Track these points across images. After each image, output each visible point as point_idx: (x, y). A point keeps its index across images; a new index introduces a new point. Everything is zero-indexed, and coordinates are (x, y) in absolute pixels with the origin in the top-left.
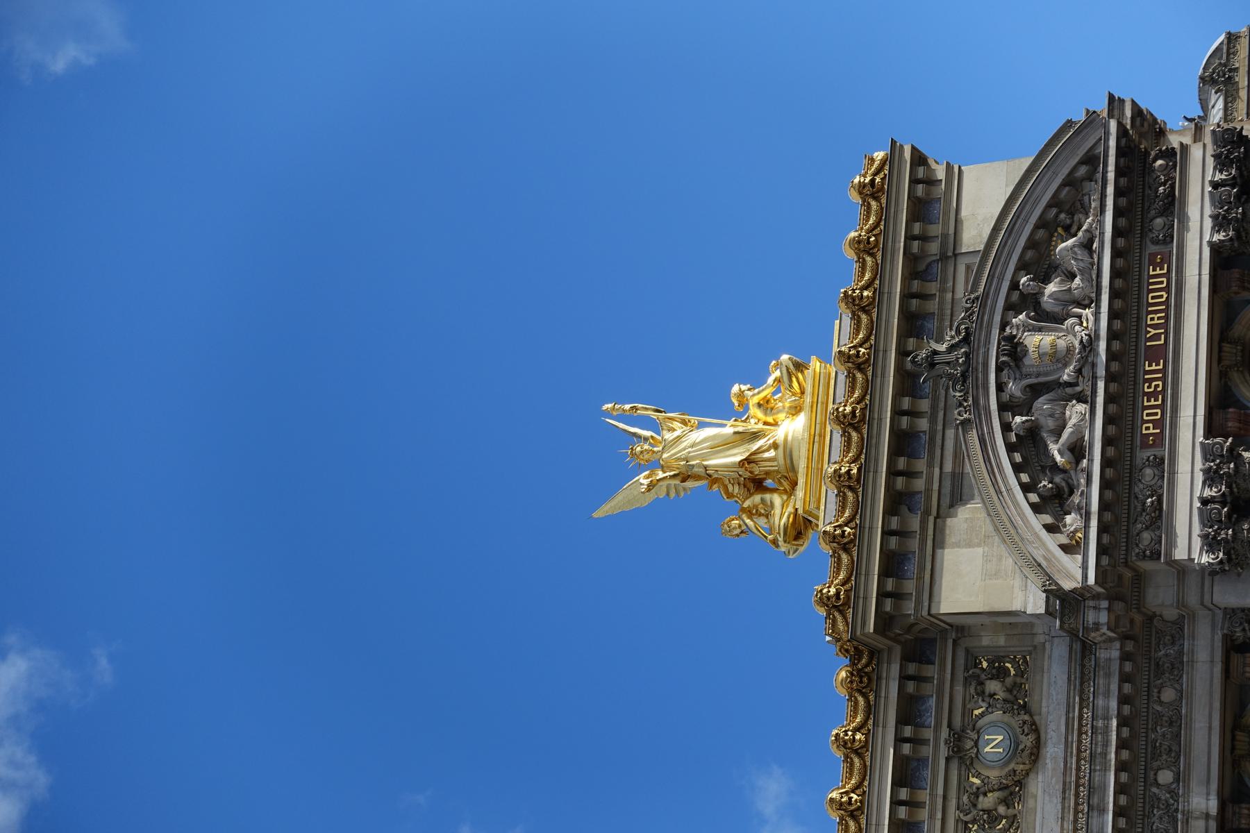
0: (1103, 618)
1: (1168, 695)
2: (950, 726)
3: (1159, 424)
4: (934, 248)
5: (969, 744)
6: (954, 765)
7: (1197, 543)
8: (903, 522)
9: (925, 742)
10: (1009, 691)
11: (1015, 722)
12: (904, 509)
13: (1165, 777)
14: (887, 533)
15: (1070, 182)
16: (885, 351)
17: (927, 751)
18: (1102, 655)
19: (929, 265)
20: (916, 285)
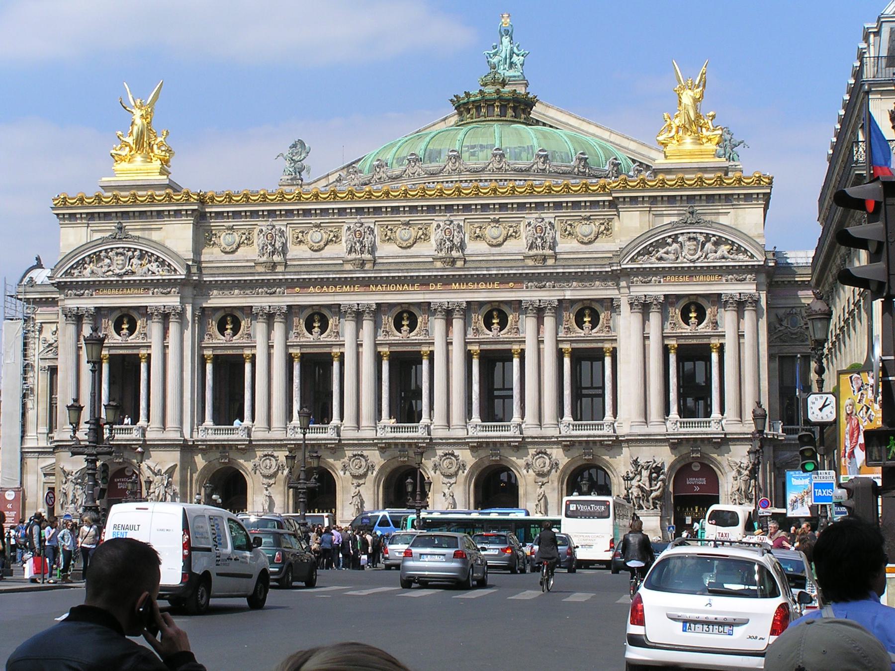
0: (615, 268)
4: (735, 203)
10: (602, 232)
11: (592, 236)
13: (575, 284)
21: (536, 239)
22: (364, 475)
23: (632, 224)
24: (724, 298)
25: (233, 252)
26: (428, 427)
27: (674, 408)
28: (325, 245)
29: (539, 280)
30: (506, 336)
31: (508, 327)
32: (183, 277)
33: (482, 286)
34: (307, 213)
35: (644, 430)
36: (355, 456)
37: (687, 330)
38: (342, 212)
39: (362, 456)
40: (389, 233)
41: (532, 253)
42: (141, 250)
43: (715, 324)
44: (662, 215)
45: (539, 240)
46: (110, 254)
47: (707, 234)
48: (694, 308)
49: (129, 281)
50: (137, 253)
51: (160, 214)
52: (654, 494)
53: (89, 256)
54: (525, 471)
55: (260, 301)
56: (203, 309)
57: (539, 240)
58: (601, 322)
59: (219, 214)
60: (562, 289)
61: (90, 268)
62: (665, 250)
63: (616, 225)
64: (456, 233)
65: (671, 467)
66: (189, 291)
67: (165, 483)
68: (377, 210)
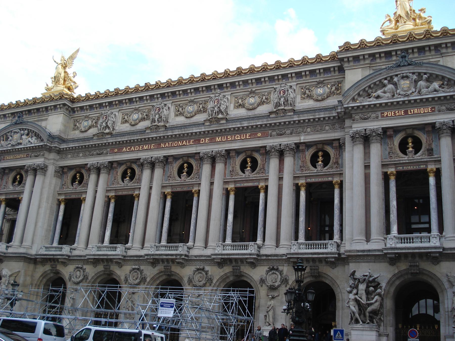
0: (339, 111)
1: (327, 128)
2: (324, 80)
3: (387, 116)
5: (320, 85)
6: (316, 83)
7: (355, 129)
8: (367, 58)
9: (320, 75)
10: (333, 92)
12: (372, 58)
13: (309, 130)
14: (364, 55)
16: (412, 44)
17: (318, 76)
18: (334, 112)
19: (439, 50)
20: (432, 48)
21: (280, 99)
23: (354, 76)
24: (437, 125)
25: (86, 131)
26: (189, 248)
27: (394, 229)
28: (140, 122)
29: (279, 129)
31: (257, 169)
33: (238, 137)
34: (131, 100)
36: (134, 269)
37: (405, 158)
38: (152, 97)
39: (138, 269)
40: (180, 109)
42: (28, 129)
43: (430, 151)
45: (282, 99)
47: (419, 73)
48: (410, 140)
49: (18, 149)
50: (26, 132)
51: (46, 108)
52: (369, 309)
54: (259, 286)
55: (92, 161)
56: (63, 168)
57: (282, 99)
58: (331, 161)
59: (82, 108)
60: (298, 134)
64: (222, 102)
65: (390, 283)
66: (52, 156)
68: (174, 93)
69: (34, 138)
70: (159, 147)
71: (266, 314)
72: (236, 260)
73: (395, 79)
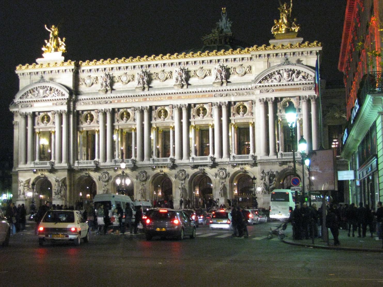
15: (311, 76)
22: (145, 180)
30: (206, 118)
32: (68, 97)
35: (267, 158)
39: (144, 172)
41: (216, 81)
44: (273, 62)
46: (38, 89)
52: (271, 187)
53: (30, 90)
54: (215, 178)
56: (78, 111)
61: (30, 95)
62: (275, 77)
63: (253, 68)
67: (60, 185)
69: (56, 93)
70: (145, 100)
71: (220, 191)
72: (201, 166)
73: (281, 72)
